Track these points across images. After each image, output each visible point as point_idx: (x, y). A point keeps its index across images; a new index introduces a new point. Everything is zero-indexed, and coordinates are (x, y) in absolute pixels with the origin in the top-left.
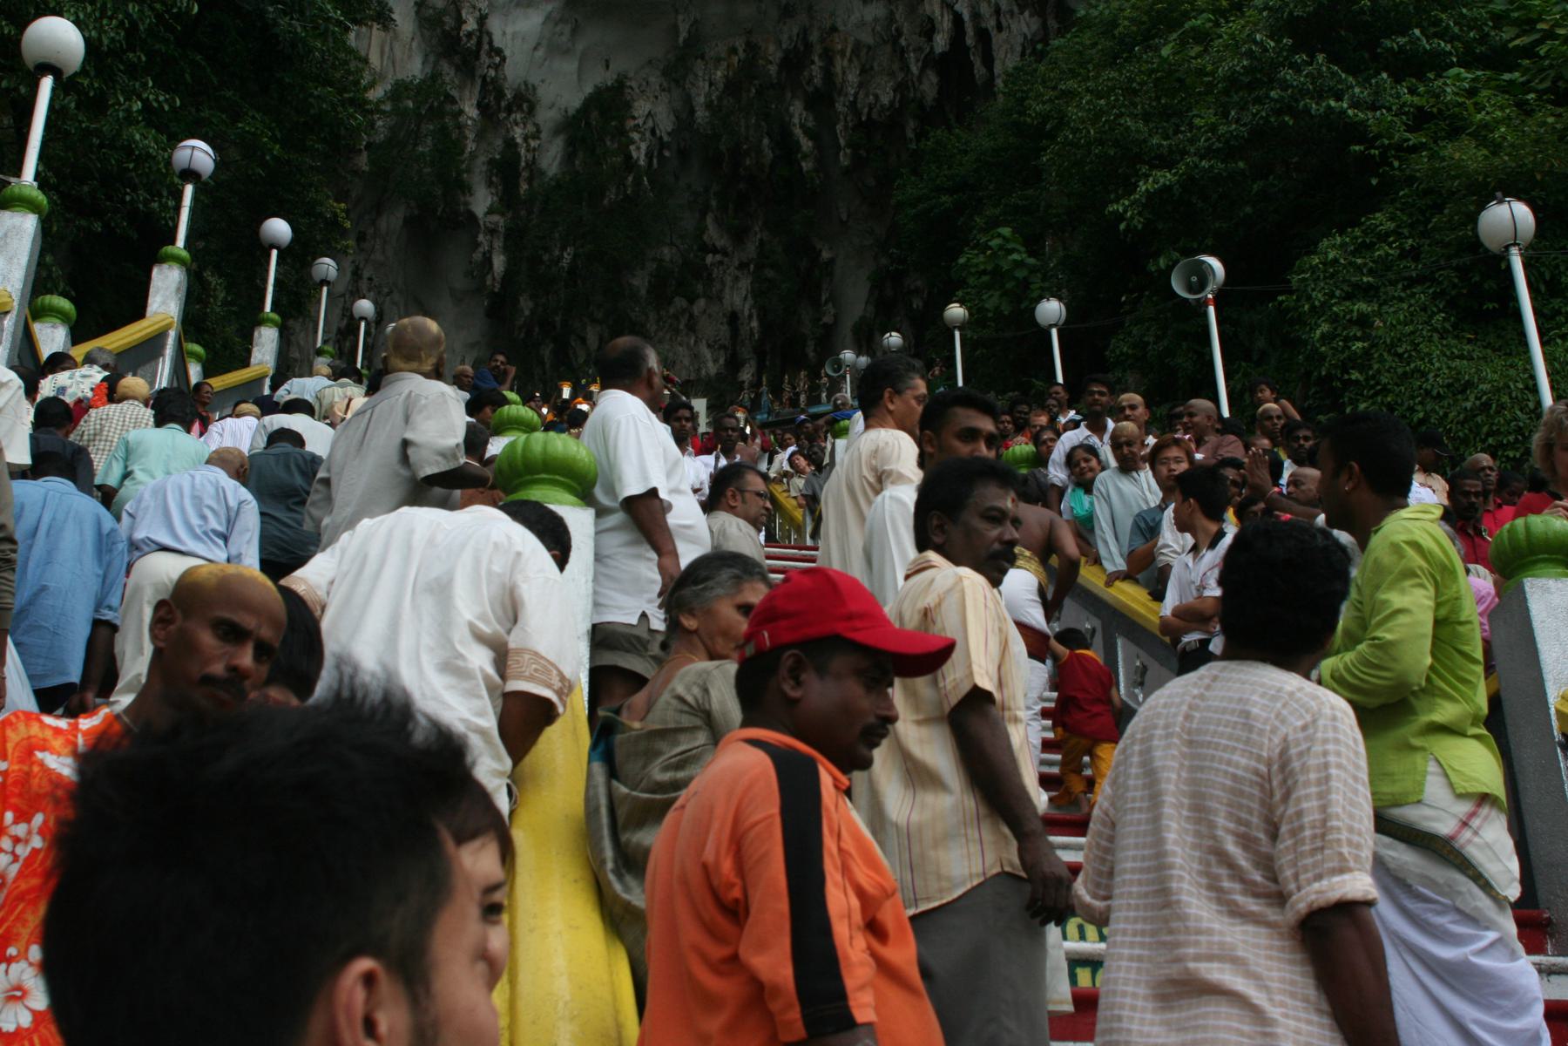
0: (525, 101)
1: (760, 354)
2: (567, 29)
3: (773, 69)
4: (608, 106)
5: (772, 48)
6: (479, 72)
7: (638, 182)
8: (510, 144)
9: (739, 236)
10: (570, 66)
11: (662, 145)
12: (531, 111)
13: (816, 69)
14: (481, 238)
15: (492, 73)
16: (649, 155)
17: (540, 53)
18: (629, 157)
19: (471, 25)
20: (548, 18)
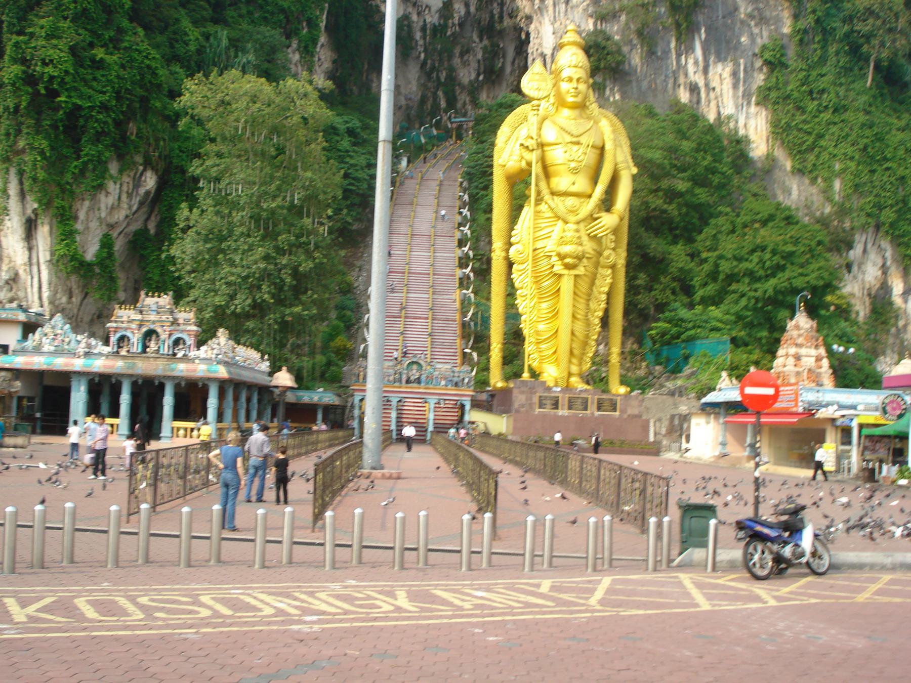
1: (484, 72)
8: (425, 21)
9: (481, 40)
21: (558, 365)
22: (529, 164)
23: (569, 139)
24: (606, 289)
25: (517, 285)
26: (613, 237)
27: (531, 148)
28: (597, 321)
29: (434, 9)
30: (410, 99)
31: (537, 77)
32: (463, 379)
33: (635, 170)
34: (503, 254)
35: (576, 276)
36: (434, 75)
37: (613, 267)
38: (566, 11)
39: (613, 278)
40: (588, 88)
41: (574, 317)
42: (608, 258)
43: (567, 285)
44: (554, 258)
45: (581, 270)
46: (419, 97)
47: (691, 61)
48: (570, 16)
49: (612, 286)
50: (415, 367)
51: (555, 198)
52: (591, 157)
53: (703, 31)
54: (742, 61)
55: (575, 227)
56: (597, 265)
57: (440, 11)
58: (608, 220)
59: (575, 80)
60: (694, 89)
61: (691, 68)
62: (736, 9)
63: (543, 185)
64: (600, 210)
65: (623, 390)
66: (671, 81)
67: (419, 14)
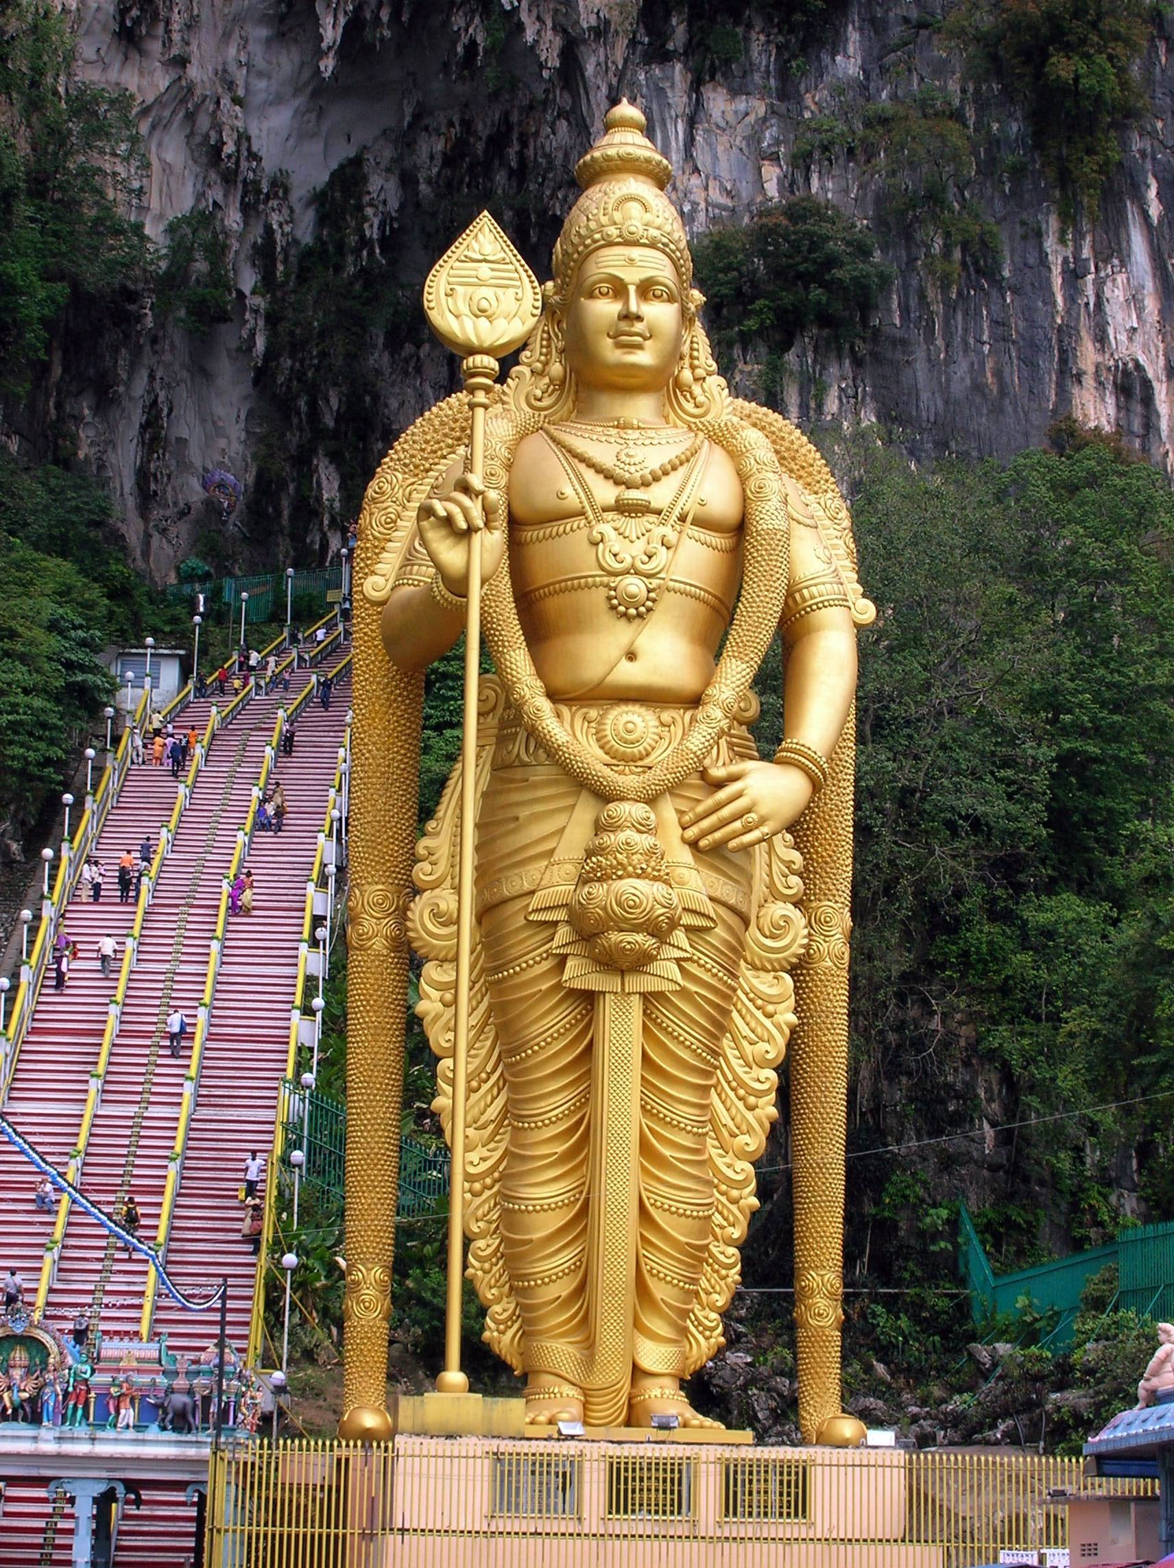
0: (280, 186)
2: (313, 116)
3: (480, 147)
4: (349, 178)
5: (480, 127)
6: (240, 178)
7: (371, 253)
8: (269, 231)
10: (317, 147)
11: (392, 219)
12: (286, 191)
13: (512, 152)
14: (247, 316)
15: (251, 175)
16: (382, 225)
17: (291, 142)
18: (362, 236)
19: (229, 148)
20: (296, 111)
22: (458, 585)
23: (606, 493)
24: (775, 1050)
25: (438, 1038)
26: (796, 856)
27: (464, 526)
29: (299, 192)
30: (221, 485)
31: (484, 271)
33: (867, 611)
34: (387, 927)
35: (648, 998)
36: (302, 404)
37: (800, 969)
38: (690, 141)
39: (795, 1011)
40: (685, 318)
44: (563, 934)
45: (665, 973)
46: (250, 478)
47: (1116, 293)
48: (702, 157)
50: (19, 1355)
51: (565, 710)
52: (694, 561)
53: (1152, 193)
55: (638, 810)
57: (320, 199)
58: (772, 788)
59: (632, 289)
60: (1130, 387)
61: (1119, 318)
63: (519, 661)
65: (848, 1427)
66: (1049, 365)
67: (246, 209)
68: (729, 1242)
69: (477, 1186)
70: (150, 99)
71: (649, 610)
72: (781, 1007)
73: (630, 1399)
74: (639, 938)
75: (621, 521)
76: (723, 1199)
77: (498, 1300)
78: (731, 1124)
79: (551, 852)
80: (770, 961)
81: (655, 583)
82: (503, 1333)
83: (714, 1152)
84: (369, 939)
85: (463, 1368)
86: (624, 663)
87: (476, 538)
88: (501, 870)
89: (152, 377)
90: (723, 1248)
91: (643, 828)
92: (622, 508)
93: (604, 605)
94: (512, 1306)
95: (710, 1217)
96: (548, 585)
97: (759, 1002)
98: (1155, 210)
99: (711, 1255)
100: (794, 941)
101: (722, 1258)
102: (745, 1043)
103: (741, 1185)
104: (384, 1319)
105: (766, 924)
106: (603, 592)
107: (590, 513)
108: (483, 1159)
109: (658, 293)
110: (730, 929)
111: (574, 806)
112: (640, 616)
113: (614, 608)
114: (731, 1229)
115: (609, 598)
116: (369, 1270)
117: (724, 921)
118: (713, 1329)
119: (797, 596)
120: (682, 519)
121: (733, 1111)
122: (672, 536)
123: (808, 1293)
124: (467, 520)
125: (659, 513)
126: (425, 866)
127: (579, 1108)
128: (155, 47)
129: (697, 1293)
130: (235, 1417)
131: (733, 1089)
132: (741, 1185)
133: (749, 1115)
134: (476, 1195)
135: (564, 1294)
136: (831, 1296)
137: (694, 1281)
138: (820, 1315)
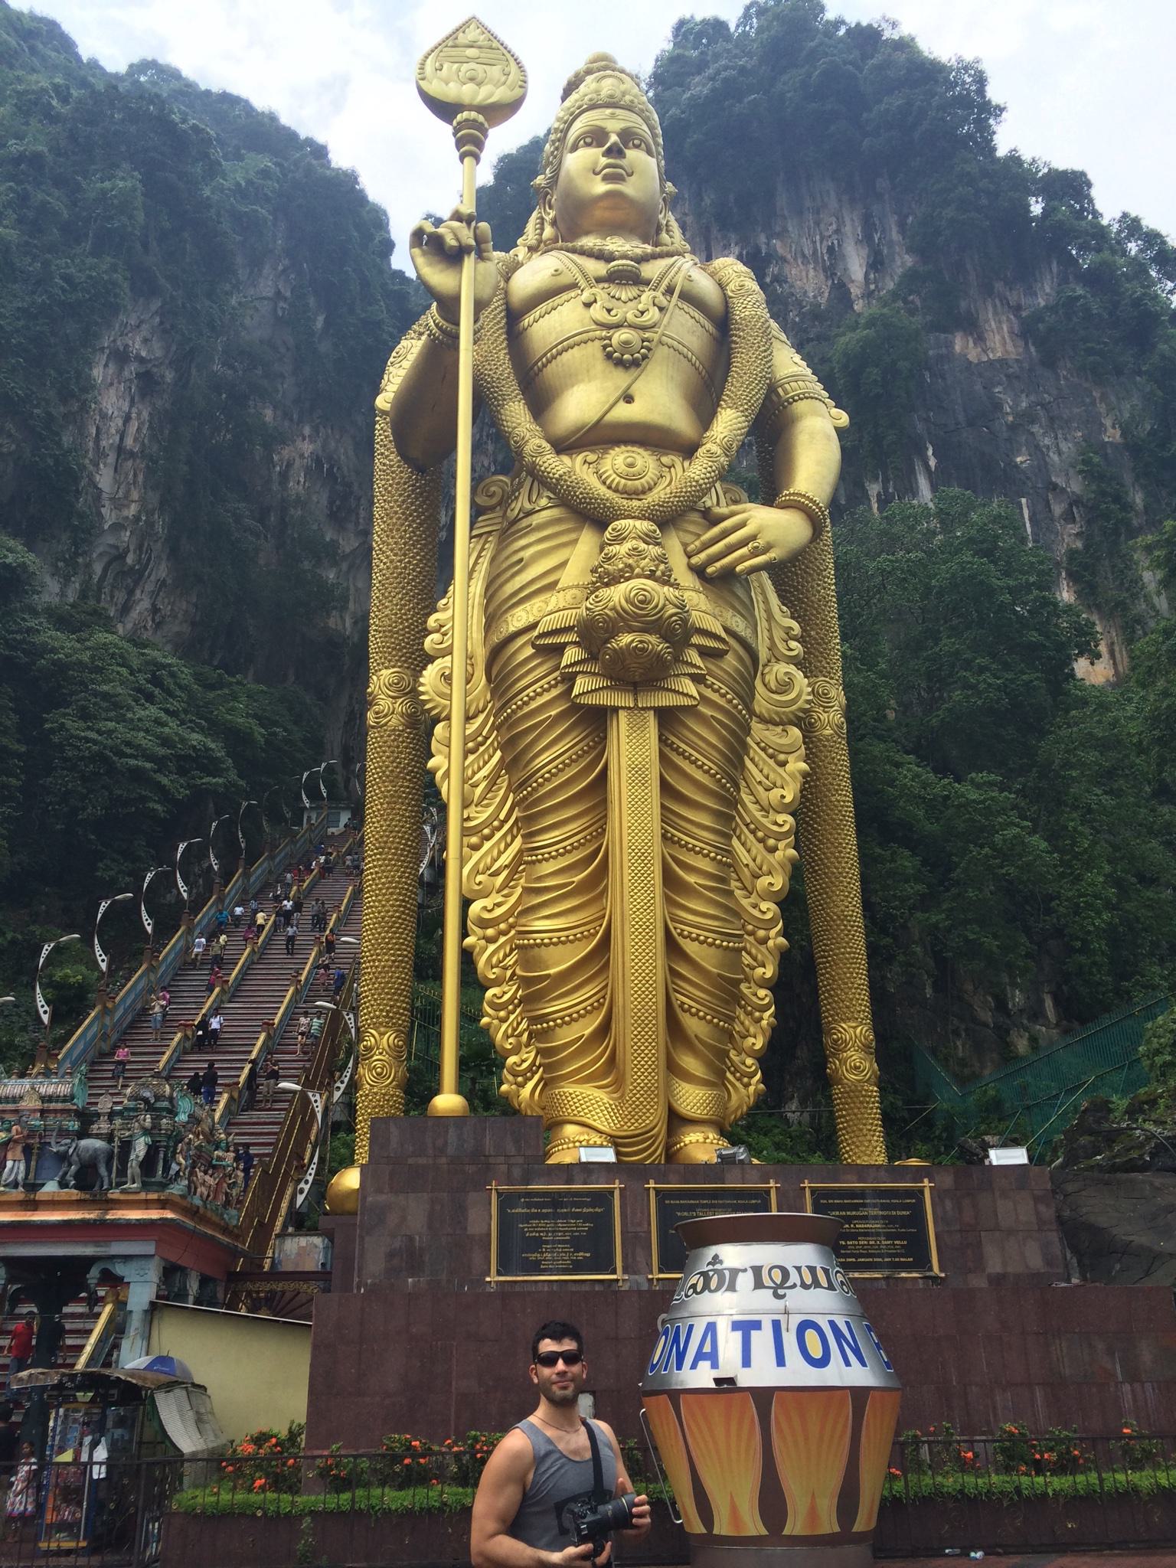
21: (618, 1085)
23: (599, 268)
28: (769, 909)
32: (127, 1146)
41: (671, 880)
42: (785, 686)
43: (633, 747)
49: (811, 786)
51: (566, 459)
52: (686, 330)
53: (930, 452)
54: (1024, 501)
55: (644, 526)
56: (747, 696)
58: (774, 526)
62: (998, 406)
63: (516, 415)
64: (736, 502)
68: (763, 983)
69: (490, 932)
70: (348, 550)
71: (645, 357)
72: (791, 758)
73: (668, 1147)
74: (653, 639)
75: (614, 290)
76: (751, 939)
77: (516, 1050)
78: (751, 864)
79: (556, 583)
80: (777, 713)
81: (647, 335)
82: (522, 1085)
83: (738, 893)
84: (385, 716)
85: (459, 1092)
86: (622, 405)
87: (469, 262)
88: (506, 611)
89: (351, 697)
90: (754, 988)
91: (648, 538)
92: (612, 278)
93: (600, 355)
94: (533, 1054)
95: (739, 951)
96: (545, 354)
97: (771, 751)
98: (932, 462)
99: (743, 997)
100: (799, 696)
101: (754, 999)
102: (760, 788)
103: (769, 924)
104: (397, 1087)
105: (771, 679)
106: (598, 344)
107: (583, 283)
108: (499, 905)
109: (637, 142)
110: (740, 659)
111: (576, 541)
112: (635, 364)
113: (609, 357)
114: (760, 971)
115: (605, 347)
116: (382, 1034)
117: (736, 651)
118: (752, 1075)
119: (780, 390)
120: (670, 291)
121: (754, 851)
122: (662, 300)
123: (839, 1047)
124: (458, 239)
125: (647, 283)
126: (436, 637)
127: (595, 837)
128: (351, 526)
129: (731, 1036)
130: (167, 1168)
131: (753, 832)
132: (769, 924)
133: (769, 857)
134: (491, 940)
135: (587, 1032)
136: (866, 1048)
137: (731, 1019)
138: (856, 1068)
